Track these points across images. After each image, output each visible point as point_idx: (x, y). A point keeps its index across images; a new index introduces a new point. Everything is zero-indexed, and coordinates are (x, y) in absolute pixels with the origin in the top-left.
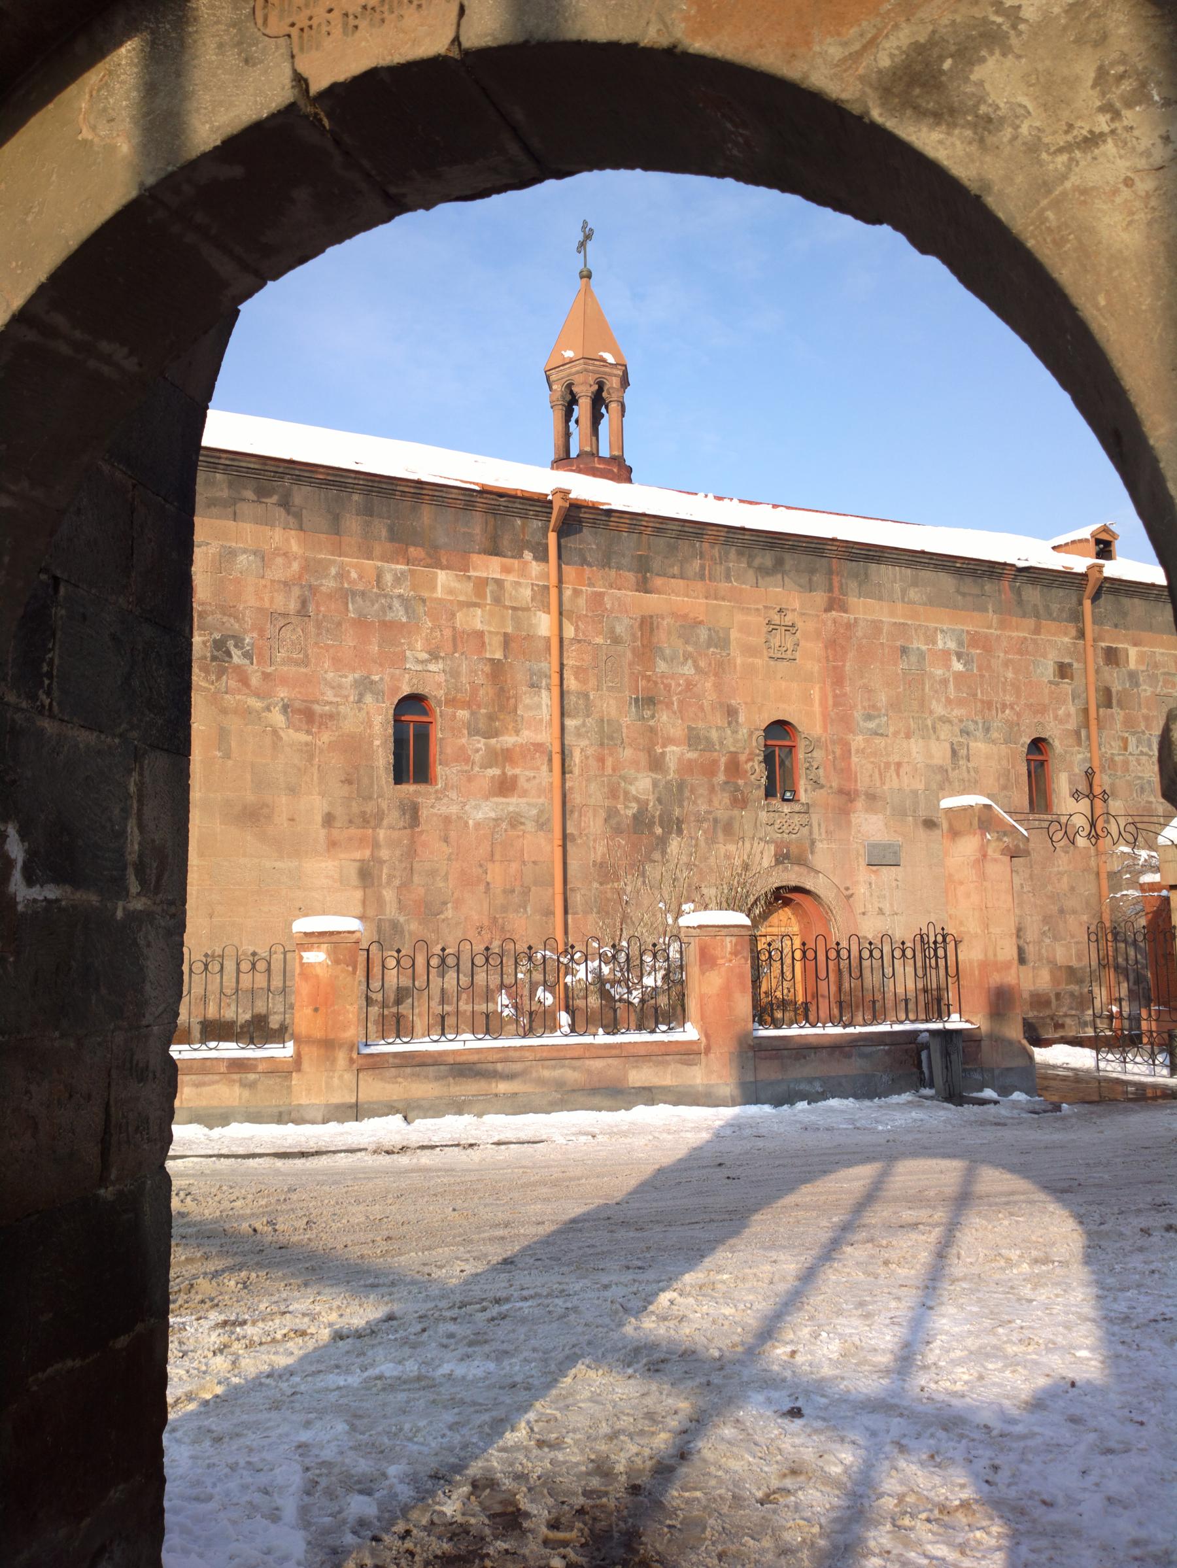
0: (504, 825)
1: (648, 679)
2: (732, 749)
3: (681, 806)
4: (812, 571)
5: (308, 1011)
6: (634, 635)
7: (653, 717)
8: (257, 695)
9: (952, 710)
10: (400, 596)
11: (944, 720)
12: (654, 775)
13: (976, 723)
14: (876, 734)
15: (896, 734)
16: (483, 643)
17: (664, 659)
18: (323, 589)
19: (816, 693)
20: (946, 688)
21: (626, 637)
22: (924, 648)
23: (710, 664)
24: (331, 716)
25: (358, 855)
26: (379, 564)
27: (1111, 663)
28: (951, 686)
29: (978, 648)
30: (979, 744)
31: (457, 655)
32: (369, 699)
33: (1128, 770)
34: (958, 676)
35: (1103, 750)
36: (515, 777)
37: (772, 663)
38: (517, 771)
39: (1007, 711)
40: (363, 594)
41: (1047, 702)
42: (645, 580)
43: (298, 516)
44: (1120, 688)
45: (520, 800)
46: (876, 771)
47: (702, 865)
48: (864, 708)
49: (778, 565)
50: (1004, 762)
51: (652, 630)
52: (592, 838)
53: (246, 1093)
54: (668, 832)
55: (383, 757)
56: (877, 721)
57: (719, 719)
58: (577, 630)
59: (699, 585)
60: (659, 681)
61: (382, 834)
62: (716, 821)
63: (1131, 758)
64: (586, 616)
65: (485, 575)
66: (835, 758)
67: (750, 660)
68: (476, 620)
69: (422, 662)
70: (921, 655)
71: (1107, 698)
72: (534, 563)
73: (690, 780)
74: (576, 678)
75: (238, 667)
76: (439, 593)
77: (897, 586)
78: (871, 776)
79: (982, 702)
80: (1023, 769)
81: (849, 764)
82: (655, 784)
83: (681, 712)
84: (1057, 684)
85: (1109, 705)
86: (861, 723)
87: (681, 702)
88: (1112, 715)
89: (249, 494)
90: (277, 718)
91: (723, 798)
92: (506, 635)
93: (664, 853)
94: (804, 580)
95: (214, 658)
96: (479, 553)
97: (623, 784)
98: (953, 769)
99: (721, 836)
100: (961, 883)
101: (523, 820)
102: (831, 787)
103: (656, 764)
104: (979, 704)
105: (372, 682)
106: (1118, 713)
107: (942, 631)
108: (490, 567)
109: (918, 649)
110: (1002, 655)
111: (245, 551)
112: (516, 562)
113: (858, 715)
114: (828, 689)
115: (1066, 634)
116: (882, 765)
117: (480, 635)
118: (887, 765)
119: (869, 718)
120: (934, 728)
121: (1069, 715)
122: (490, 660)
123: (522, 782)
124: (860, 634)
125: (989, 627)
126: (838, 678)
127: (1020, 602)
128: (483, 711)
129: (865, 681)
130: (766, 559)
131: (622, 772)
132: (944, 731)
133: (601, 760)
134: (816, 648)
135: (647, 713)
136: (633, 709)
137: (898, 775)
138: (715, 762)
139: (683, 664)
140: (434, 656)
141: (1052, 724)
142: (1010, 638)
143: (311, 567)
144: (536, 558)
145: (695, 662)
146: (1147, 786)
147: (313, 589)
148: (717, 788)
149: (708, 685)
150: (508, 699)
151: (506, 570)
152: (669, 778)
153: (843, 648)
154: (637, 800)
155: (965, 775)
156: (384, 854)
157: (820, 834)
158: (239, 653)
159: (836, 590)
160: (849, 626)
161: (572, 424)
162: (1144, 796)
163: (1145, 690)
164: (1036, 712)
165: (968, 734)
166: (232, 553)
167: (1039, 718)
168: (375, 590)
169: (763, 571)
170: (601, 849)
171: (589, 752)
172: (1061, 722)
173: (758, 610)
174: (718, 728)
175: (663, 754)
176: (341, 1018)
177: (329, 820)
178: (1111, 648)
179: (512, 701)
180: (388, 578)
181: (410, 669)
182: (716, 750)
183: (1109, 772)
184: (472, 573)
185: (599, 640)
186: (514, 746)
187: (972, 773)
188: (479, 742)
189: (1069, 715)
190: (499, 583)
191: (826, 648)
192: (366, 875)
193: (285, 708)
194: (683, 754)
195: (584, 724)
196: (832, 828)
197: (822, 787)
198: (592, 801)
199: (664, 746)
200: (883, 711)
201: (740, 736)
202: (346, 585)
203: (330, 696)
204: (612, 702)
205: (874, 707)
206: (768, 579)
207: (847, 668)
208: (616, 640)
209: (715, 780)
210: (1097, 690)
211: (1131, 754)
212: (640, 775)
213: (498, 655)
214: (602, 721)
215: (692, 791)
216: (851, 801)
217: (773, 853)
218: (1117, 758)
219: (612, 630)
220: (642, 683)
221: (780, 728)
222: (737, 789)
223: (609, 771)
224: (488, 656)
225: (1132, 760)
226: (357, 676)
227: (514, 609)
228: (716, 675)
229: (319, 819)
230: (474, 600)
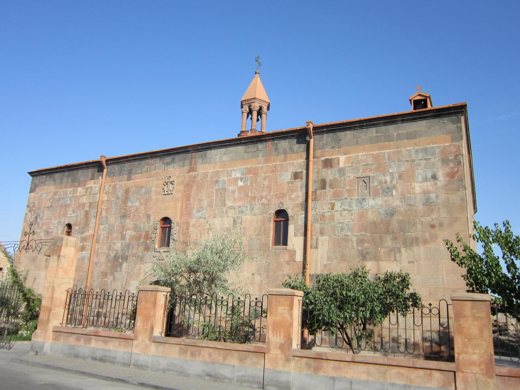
0: (80, 261)
1: (125, 209)
2: (147, 230)
3: (128, 252)
4: (185, 160)
6: (123, 195)
7: (124, 222)
9: (236, 203)
11: (232, 208)
12: (122, 241)
13: (247, 207)
14: (201, 218)
15: (209, 216)
16: (85, 206)
17: (130, 202)
18: (56, 199)
19: (179, 205)
20: (234, 193)
21: (121, 197)
22: (225, 179)
23: (144, 201)
24: (51, 232)
27: (327, 167)
28: (237, 193)
29: (251, 174)
30: (247, 216)
32: (59, 226)
33: (333, 220)
34: (241, 188)
35: (318, 211)
36: (86, 245)
37: (165, 196)
39: (263, 200)
40: (63, 198)
41: (285, 192)
42: (130, 177)
43: (55, 181)
44: (332, 178)
45: (86, 252)
46: (199, 233)
47: (131, 273)
48: (197, 208)
49: (173, 161)
50: (259, 224)
51: (128, 192)
52: (102, 263)
54: (123, 261)
56: (202, 213)
57: (144, 220)
58: (108, 197)
59: (145, 175)
60: (128, 209)
62: (138, 256)
63: (335, 213)
64: (111, 192)
66: (183, 229)
69: (71, 214)
70: (224, 182)
71: (323, 184)
73: (133, 242)
74: (105, 213)
76: (78, 194)
77: (218, 157)
78: (197, 235)
79: (251, 197)
80: (272, 225)
81: (188, 231)
82: (122, 245)
83: (133, 219)
84: (292, 183)
85: (324, 187)
86: (196, 214)
87: (133, 215)
88: (325, 193)
89: (48, 179)
91: (141, 248)
93: (121, 268)
94: (181, 164)
96: (89, 180)
97: (113, 246)
98: (233, 229)
99: (139, 261)
101: (85, 258)
102: (180, 241)
103: (123, 238)
104: (249, 199)
105: (60, 222)
106: (329, 191)
107: (235, 170)
109: (223, 180)
110: (263, 175)
111: (44, 193)
113: (194, 211)
115: (301, 158)
116: (202, 230)
117: (84, 204)
118: (205, 229)
119: (199, 211)
120: (226, 212)
121: (298, 196)
123: (87, 246)
124: (198, 179)
125: (260, 163)
126: (188, 197)
127: (276, 149)
128: (82, 226)
130: (168, 159)
131: (113, 241)
132: (231, 213)
133: (108, 238)
134: (181, 188)
135: (123, 221)
136: (119, 220)
137: (208, 234)
138: (141, 235)
139: (136, 202)
141: (288, 203)
142: (268, 166)
143: (55, 194)
145: (140, 201)
146: (346, 227)
147: (54, 199)
149: (143, 208)
150: (88, 221)
151: (94, 183)
152: (126, 242)
153: (191, 186)
154: (116, 250)
155: (239, 231)
159: (193, 164)
160: (195, 177)
162: (343, 233)
163: (349, 176)
164: (280, 197)
165: (242, 212)
166: (42, 194)
167: (280, 200)
169: (168, 164)
170: (103, 267)
171: (105, 236)
172: (293, 200)
173: (162, 178)
174: (144, 223)
175: (125, 234)
178: (328, 159)
179: (89, 222)
180: (68, 192)
182: (142, 231)
183: (320, 222)
185: (113, 199)
186: (87, 236)
187: (243, 230)
188: (79, 235)
189: (298, 196)
191: (185, 187)
194: (131, 233)
195: (105, 227)
197: (177, 241)
198: (103, 252)
199: (126, 231)
200: (205, 208)
201: (150, 225)
203: (52, 227)
204: (114, 218)
205: (201, 207)
206: (169, 166)
207: (192, 193)
208: (118, 198)
209: (140, 242)
210: (312, 181)
211: (336, 211)
212: (118, 242)
213: (88, 209)
214: (110, 225)
215: (132, 246)
216: (187, 246)
218: (325, 214)
219: (117, 195)
220: (123, 211)
221: (166, 220)
222: (147, 244)
223: (109, 241)
224: (85, 209)
225: (337, 215)
227: (93, 194)
228: (146, 204)
229: (45, 260)
230: (85, 194)
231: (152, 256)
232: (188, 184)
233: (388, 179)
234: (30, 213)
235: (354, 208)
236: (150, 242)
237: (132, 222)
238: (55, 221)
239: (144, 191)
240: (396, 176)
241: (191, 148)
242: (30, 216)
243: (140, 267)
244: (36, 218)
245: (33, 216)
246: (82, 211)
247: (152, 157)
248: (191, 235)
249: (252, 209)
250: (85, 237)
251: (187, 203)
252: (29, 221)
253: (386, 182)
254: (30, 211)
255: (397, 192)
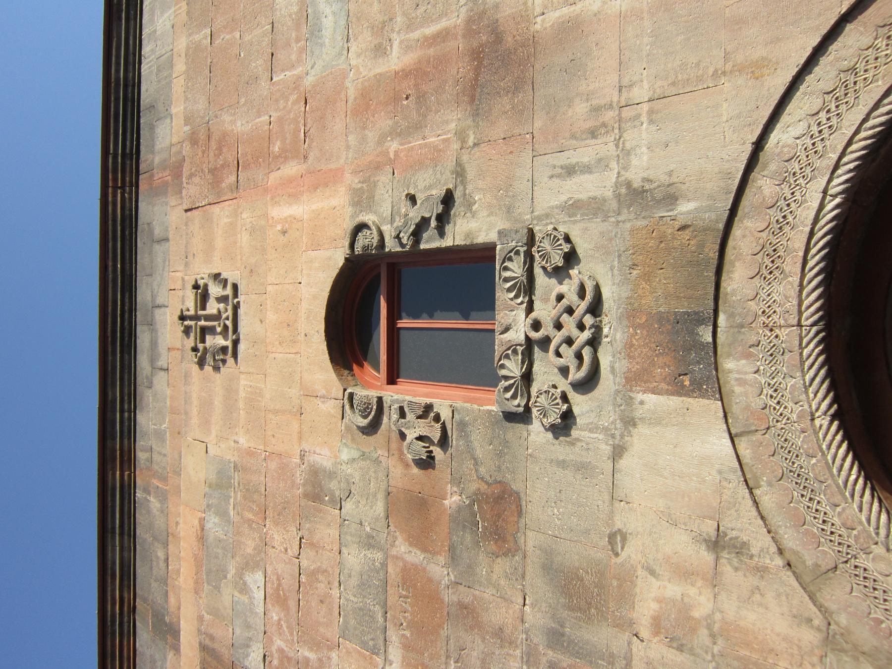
2: (380, 507)
23: (250, 522)
37: (241, 347)
66: (395, 133)
67: (241, 405)
114: (274, 177)
129: (259, 65)
139: (251, 598)
148: (466, 595)
157: (602, 163)
182: (384, 565)
196: (581, 108)
197: (460, 172)
209: (449, 597)
217: (675, 401)
231: (560, 449)
232: (211, 171)
236: (457, 481)
237: (334, 655)
239: (217, 520)
241: (115, 196)
243: (657, 625)
247: (128, 459)
248: (430, 30)
251: (277, 149)
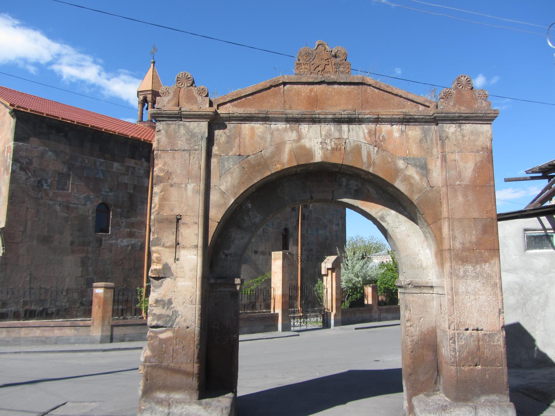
5: (97, 307)
8: (51, 200)
10: (101, 170)
24: (76, 208)
25: (81, 255)
26: (95, 159)
31: (118, 190)
32: (88, 203)
36: (135, 232)
38: (135, 230)
39: (278, 220)
53: (76, 332)
55: (91, 223)
61: (90, 249)
65: (129, 165)
68: (126, 179)
72: (145, 162)
75: (46, 189)
76: (114, 170)
90: (58, 208)
92: (135, 185)
95: (38, 186)
100: (276, 273)
108: (131, 163)
112: (139, 162)
117: (126, 184)
122: (130, 193)
123: (136, 234)
128: (126, 209)
140: (111, 190)
144: (146, 161)
151: (136, 164)
156: (90, 256)
158: (46, 185)
161: (145, 109)
163: (313, 216)
165: (268, 225)
168: (93, 167)
176: (107, 310)
177: (72, 243)
180: (98, 163)
181: (103, 194)
184: (125, 164)
190: (134, 168)
192: (84, 263)
193: (60, 205)
202: (84, 165)
213: (132, 192)
224: (129, 191)
226: (85, 195)
227: (138, 177)
233: (326, 221)
234: (23, 173)
235: (315, 234)
238: (81, 195)
240: (328, 220)
242: (24, 178)
244: (39, 182)
245: (32, 179)
246: (124, 192)
249: (273, 225)
250: (133, 223)
252: (23, 184)
253: (325, 223)
254: (21, 169)
255: (328, 229)
